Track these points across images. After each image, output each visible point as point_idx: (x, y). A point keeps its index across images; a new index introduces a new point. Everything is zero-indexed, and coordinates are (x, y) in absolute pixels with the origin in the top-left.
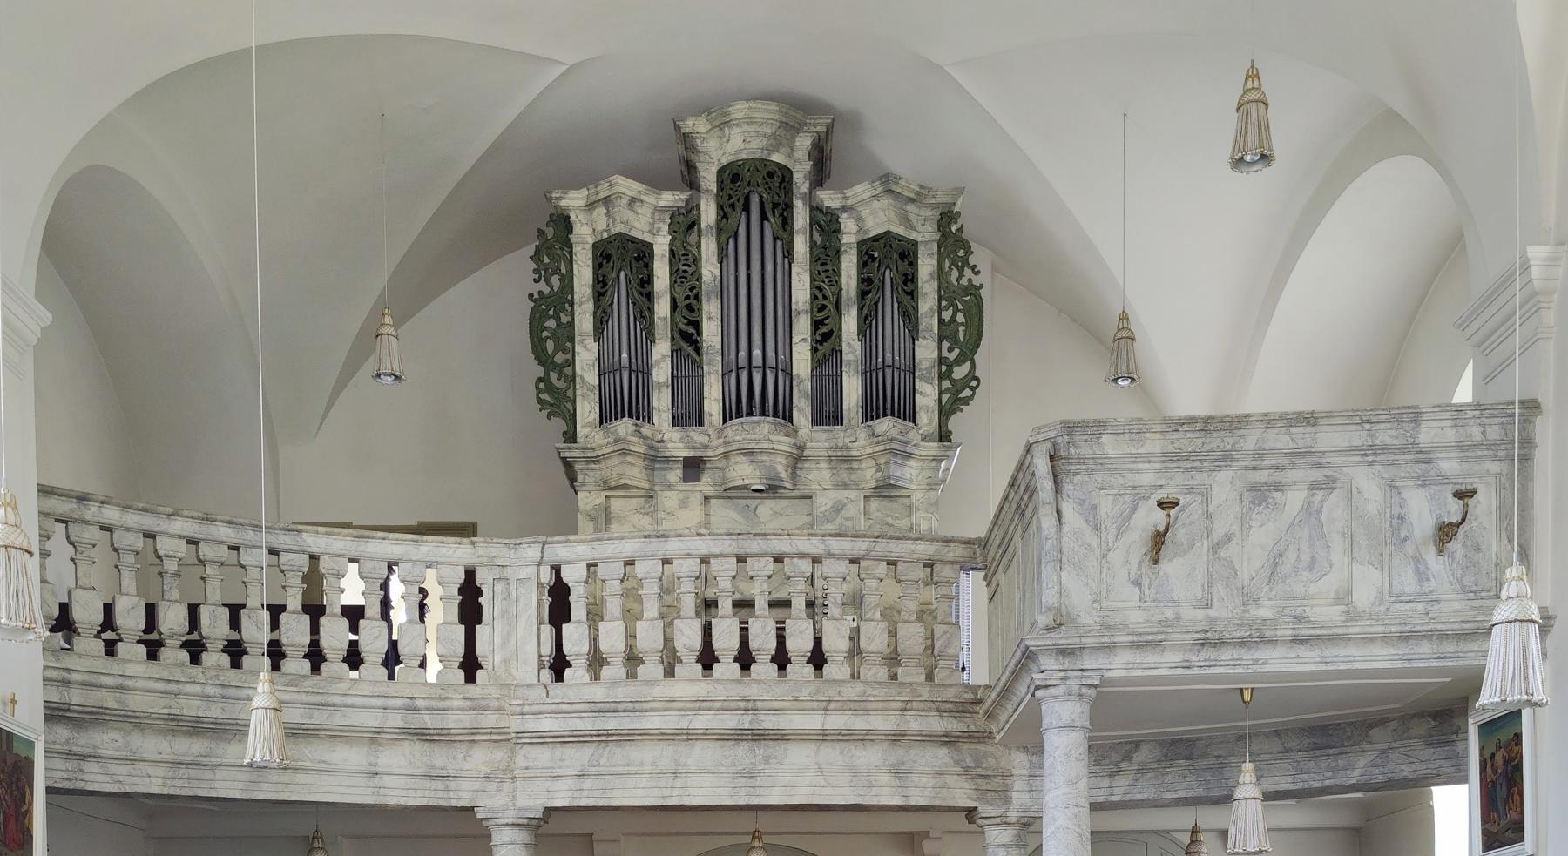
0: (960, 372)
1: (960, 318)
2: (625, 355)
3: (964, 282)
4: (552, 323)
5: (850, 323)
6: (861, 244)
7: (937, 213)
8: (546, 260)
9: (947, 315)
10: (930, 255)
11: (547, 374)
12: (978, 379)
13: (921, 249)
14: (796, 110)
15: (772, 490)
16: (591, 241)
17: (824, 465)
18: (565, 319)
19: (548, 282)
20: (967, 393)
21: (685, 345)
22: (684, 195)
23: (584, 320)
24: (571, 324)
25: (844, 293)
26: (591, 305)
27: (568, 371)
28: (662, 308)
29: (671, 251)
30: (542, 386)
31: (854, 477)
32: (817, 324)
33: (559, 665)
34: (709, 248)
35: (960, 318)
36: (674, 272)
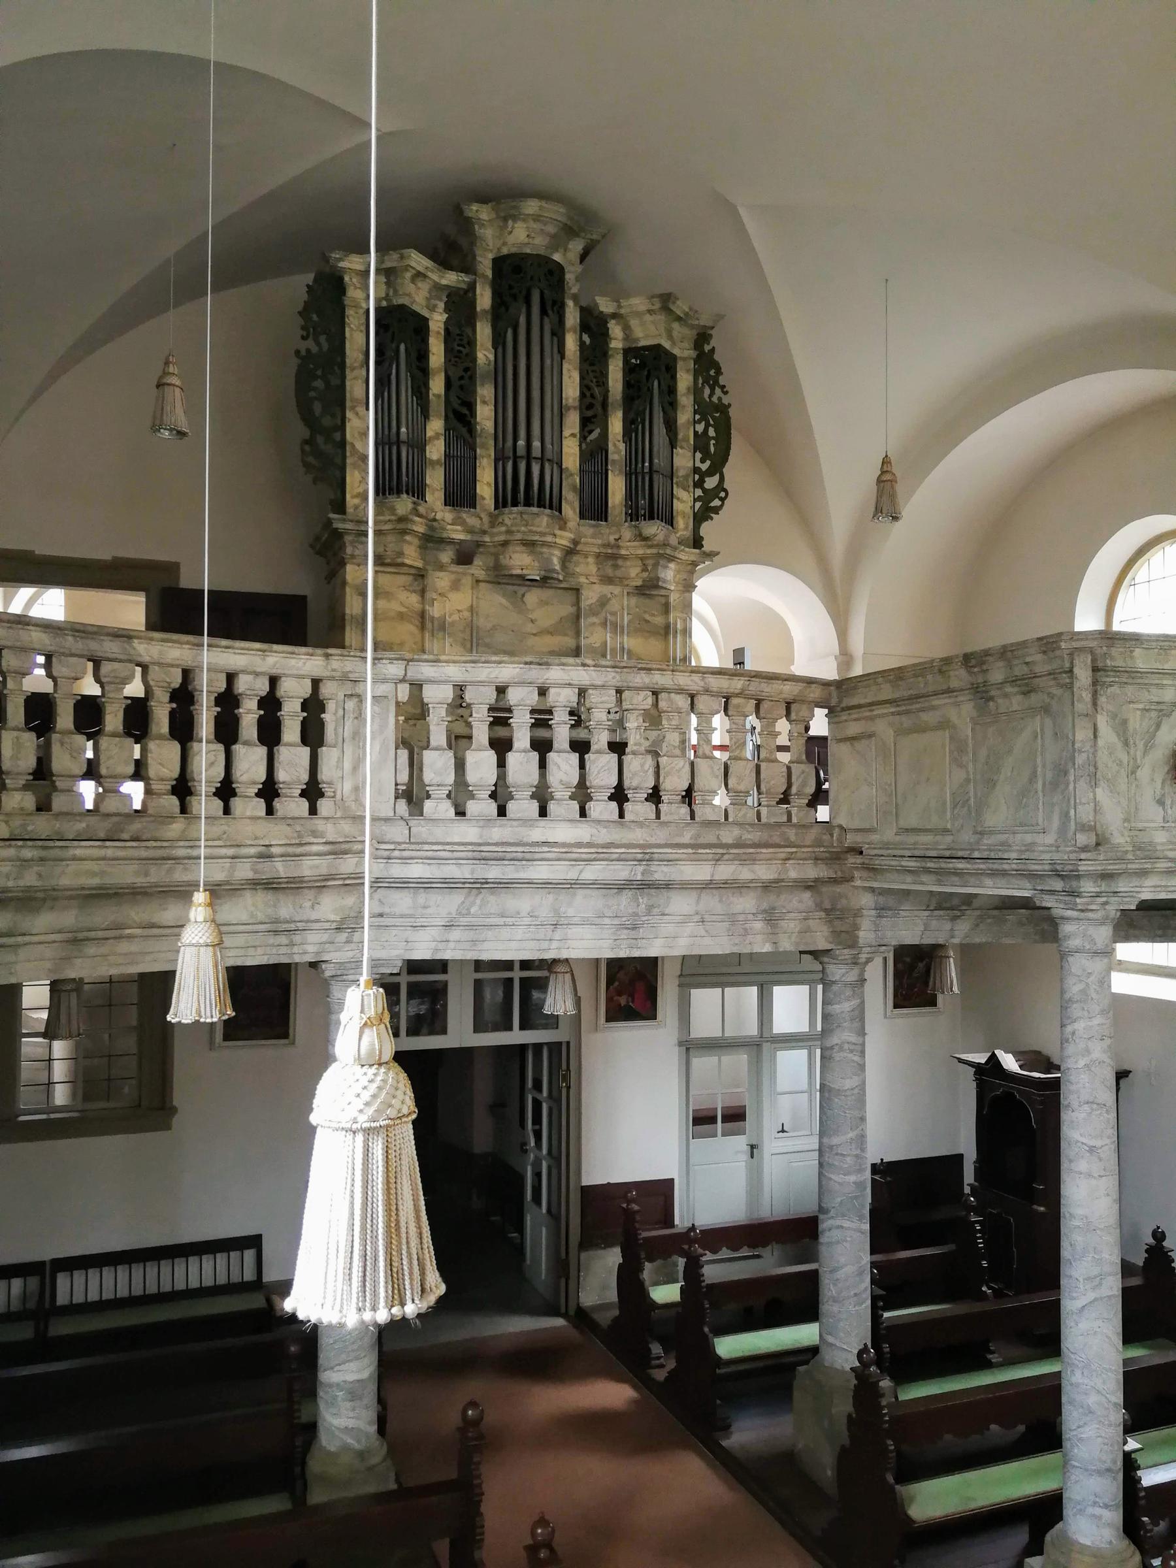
0: (711, 483)
1: (712, 432)
3: (715, 399)
4: (319, 384)
7: (695, 332)
9: (700, 428)
10: (688, 371)
13: (680, 364)
15: (545, 581)
17: (591, 560)
18: (335, 381)
19: (318, 344)
21: (459, 426)
28: (437, 386)
29: (447, 330)
30: (307, 448)
31: (619, 573)
34: (483, 332)
35: (712, 432)
36: (448, 350)
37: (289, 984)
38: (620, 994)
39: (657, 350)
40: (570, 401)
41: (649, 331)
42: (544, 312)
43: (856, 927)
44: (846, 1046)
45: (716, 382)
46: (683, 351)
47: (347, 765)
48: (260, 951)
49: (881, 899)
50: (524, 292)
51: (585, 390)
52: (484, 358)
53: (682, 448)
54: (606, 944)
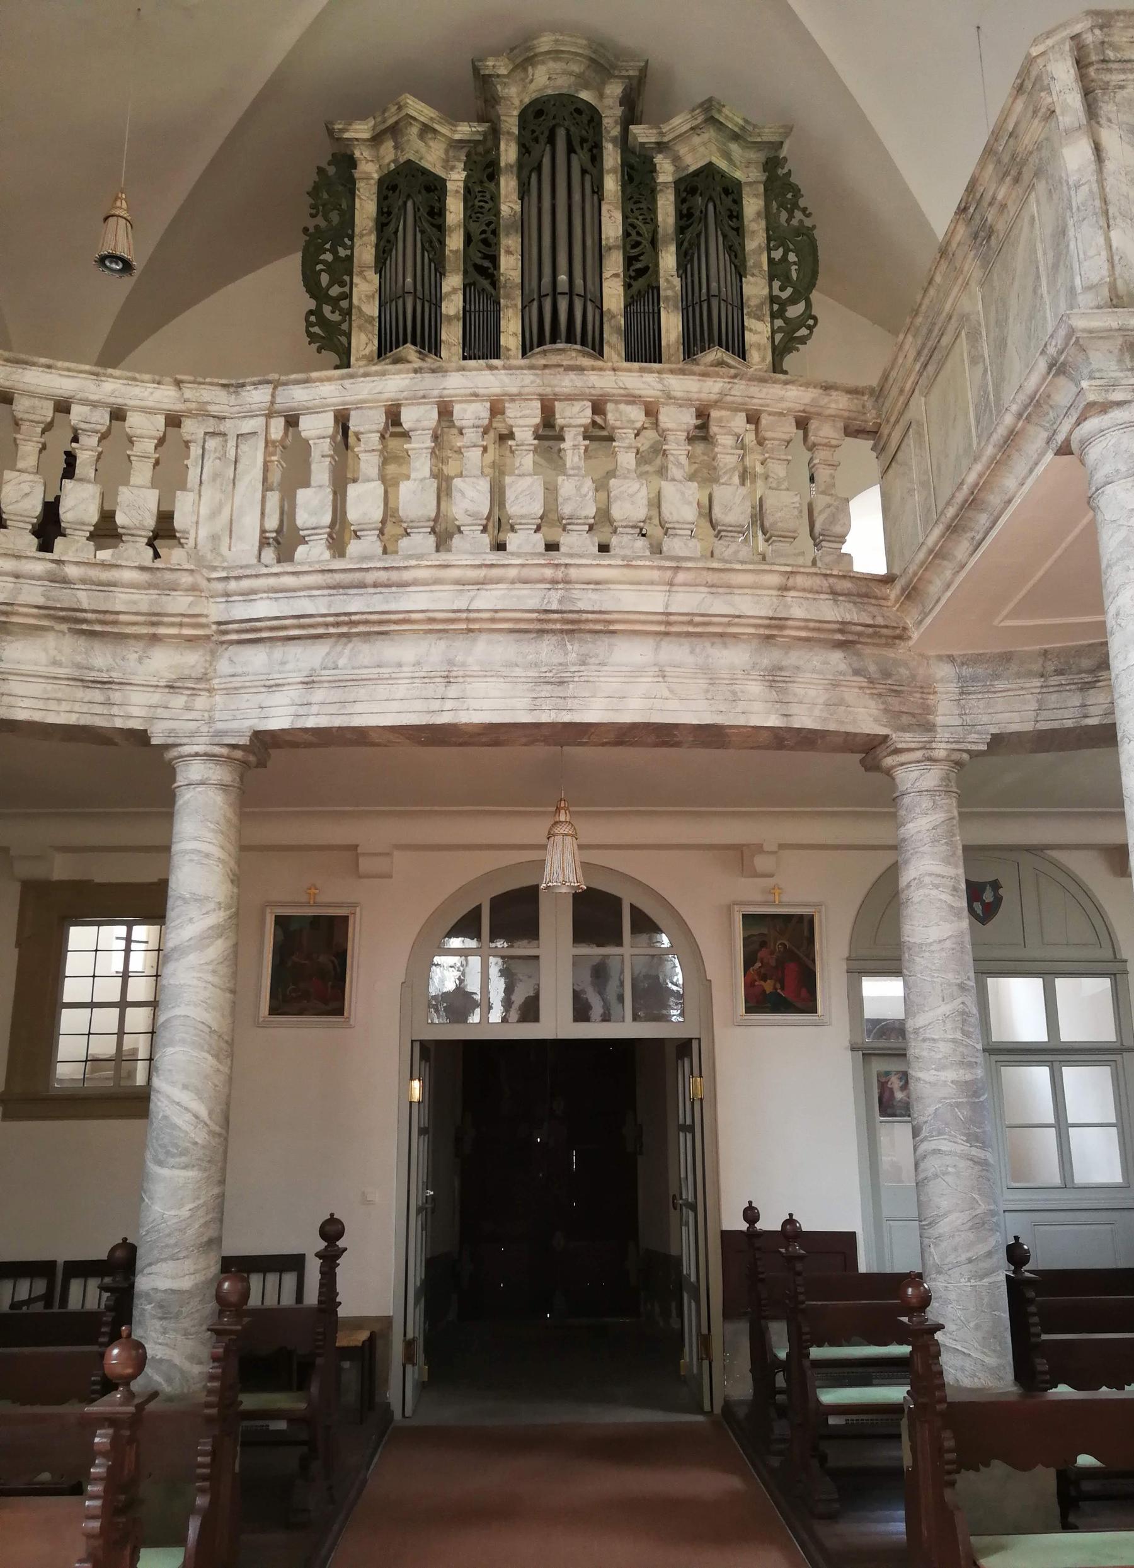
0: (795, 311)
1: (792, 257)
2: (409, 280)
3: (795, 222)
4: (328, 257)
5: (668, 260)
6: (677, 183)
8: (325, 196)
9: (777, 254)
10: (756, 196)
11: (319, 307)
12: (815, 318)
14: (601, 62)
16: (376, 176)
18: (342, 252)
20: (803, 332)
22: (481, 128)
23: (365, 251)
24: (350, 258)
25: (660, 230)
26: (373, 238)
27: (344, 304)
28: (455, 242)
30: (313, 318)
32: (629, 261)
33: (283, 541)
34: (508, 185)
35: (792, 257)
37: (345, 951)
38: (764, 978)
39: (709, 170)
40: (611, 241)
41: (698, 153)
42: (571, 150)
43: (928, 710)
44: (927, 880)
45: (795, 205)
46: (745, 170)
47: (204, 511)
48: (65, 706)
49: (966, 671)
50: (546, 133)
51: (630, 229)
52: (508, 211)
53: (753, 275)
54: (524, 702)
